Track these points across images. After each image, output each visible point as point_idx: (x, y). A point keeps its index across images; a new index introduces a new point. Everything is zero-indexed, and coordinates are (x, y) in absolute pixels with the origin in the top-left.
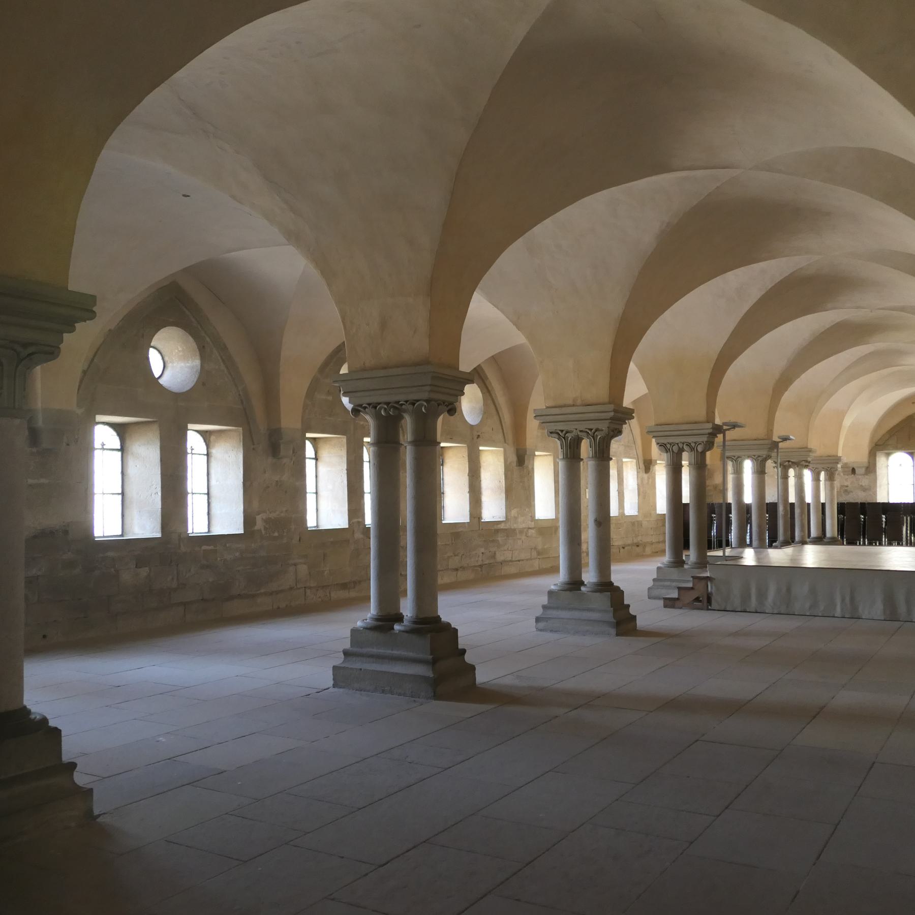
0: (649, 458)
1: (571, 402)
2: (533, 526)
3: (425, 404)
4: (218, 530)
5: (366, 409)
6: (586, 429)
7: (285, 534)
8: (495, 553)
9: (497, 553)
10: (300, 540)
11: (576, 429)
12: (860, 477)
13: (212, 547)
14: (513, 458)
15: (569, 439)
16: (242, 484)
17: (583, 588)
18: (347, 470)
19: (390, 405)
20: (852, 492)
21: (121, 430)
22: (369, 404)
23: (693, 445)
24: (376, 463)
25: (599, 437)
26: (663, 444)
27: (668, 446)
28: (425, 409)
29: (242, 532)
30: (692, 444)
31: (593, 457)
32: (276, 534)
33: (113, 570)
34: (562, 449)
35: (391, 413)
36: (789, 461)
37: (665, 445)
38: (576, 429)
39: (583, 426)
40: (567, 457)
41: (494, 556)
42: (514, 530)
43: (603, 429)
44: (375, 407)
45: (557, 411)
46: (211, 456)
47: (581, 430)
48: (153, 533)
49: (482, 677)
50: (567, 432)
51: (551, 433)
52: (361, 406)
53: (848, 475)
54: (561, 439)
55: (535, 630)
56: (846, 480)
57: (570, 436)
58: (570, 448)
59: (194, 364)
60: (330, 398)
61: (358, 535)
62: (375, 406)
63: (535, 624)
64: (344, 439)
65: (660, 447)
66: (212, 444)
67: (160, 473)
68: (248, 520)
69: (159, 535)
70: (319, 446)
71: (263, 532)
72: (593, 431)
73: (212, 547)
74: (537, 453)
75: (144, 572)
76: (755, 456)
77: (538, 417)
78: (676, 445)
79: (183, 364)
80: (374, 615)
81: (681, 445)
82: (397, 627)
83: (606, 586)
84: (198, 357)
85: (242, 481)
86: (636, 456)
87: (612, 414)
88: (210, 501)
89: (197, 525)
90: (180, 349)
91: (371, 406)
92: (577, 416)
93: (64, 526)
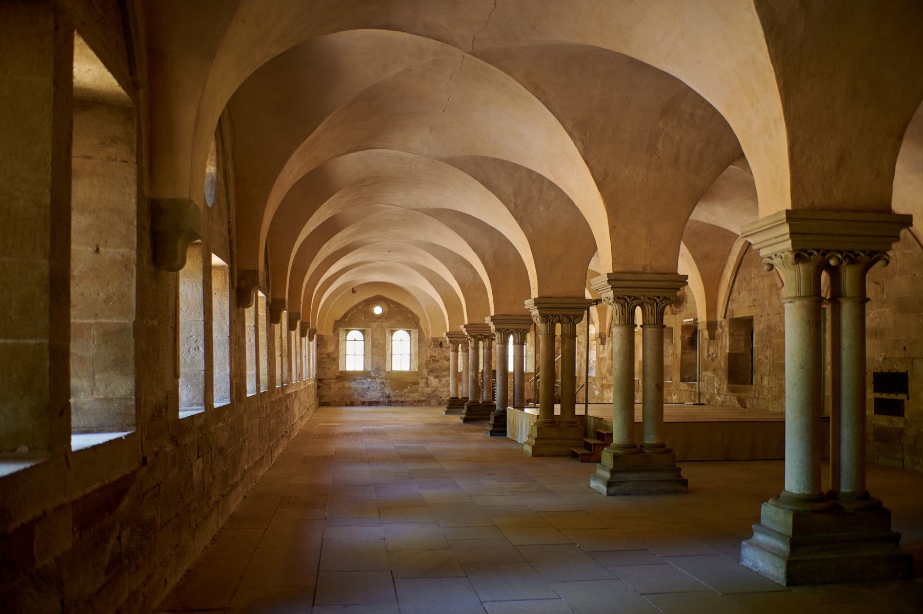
1: (640, 270)
6: (654, 296)
11: (645, 296)
12: (445, 349)
19: (844, 255)
20: (438, 361)
23: (572, 317)
24: (811, 320)
26: (546, 315)
30: (571, 317)
34: (623, 314)
36: (482, 335)
38: (645, 296)
43: (670, 297)
44: (824, 255)
45: (632, 277)
48: (192, 405)
51: (618, 298)
52: (805, 251)
53: (436, 348)
56: (435, 351)
76: (521, 329)
77: (612, 282)
78: (557, 317)
80: (809, 495)
81: (561, 317)
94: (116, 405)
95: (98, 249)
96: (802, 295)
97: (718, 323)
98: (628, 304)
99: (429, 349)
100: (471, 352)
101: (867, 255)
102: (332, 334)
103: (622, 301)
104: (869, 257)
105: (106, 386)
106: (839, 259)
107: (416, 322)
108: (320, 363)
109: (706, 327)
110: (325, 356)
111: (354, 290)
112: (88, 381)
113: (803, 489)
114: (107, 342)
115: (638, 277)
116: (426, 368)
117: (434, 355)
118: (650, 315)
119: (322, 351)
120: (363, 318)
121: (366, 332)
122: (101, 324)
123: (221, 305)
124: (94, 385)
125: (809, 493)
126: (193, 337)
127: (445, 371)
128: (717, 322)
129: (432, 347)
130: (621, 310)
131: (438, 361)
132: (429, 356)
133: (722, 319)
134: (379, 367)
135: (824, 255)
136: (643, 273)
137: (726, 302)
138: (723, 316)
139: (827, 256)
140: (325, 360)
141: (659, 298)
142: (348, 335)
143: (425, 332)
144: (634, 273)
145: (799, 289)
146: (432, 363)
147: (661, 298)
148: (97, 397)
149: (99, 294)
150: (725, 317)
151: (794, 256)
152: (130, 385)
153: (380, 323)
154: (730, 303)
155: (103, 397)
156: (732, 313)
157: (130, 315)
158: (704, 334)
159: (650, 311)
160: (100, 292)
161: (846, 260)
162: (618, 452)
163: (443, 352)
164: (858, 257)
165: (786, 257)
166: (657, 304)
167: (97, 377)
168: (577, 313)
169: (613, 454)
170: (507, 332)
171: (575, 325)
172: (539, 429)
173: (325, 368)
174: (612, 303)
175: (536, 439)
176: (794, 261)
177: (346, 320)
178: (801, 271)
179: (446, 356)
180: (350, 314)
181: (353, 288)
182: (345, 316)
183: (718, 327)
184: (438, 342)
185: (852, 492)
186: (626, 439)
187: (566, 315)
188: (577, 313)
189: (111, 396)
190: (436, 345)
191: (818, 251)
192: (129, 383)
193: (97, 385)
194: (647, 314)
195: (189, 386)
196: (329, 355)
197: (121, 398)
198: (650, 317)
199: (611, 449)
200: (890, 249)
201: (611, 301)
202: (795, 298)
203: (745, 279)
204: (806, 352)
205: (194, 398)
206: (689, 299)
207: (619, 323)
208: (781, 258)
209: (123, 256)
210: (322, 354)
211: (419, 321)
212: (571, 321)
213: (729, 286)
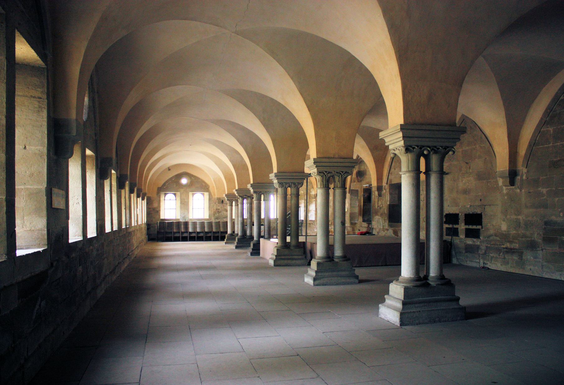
6: (340, 171)
11: (334, 171)
12: (225, 205)
16: (95, 198)
17: (336, 260)
19: (431, 148)
23: (297, 184)
24: (414, 183)
26: (281, 183)
27: (284, 184)
31: (340, 187)
36: (246, 195)
38: (334, 171)
39: (339, 170)
40: (326, 187)
44: (421, 148)
47: (337, 172)
48: (76, 236)
51: (320, 172)
52: (411, 146)
53: (219, 204)
54: (323, 177)
56: (219, 206)
65: (280, 184)
80: (413, 278)
85: (95, 196)
91: (419, 147)
92: (337, 164)
94: (36, 234)
95: (25, 147)
96: (410, 170)
97: (383, 187)
98: (325, 176)
99: (215, 205)
100: (240, 206)
101: (443, 149)
102: (156, 196)
103: (322, 174)
104: (445, 150)
105: (31, 223)
106: (428, 150)
107: (207, 189)
108: (149, 214)
109: (376, 190)
110: (152, 209)
111: (170, 168)
112: (20, 220)
113: (410, 275)
114: (31, 199)
115: (331, 160)
116: (213, 217)
117: (218, 208)
118: (338, 182)
119: (150, 207)
120: (175, 186)
121: (177, 195)
122: (27, 189)
123: (91, 178)
124: (24, 222)
126: (76, 197)
127: (225, 218)
128: (382, 186)
129: (217, 203)
130: (321, 179)
131: (221, 212)
132: (215, 209)
133: (385, 185)
134: (185, 216)
135: (421, 148)
136: (334, 158)
137: (388, 175)
138: (386, 183)
139: (423, 149)
140: (152, 212)
141: (343, 172)
142: (166, 196)
143: (212, 194)
144: (329, 158)
145: (408, 167)
146: (217, 213)
147: (344, 173)
148: (26, 229)
149: (26, 172)
150: (387, 184)
151: (405, 149)
152: (43, 223)
153: (185, 189)
154: (390, 174)
155: (29, 229)
156: (391, 181)
157: (44, 183)
158: (375, 193)
159: (338, 180)
160: (27, 171)
161: (433, 151)
162: (319, 261)
163: (224, 206)
164: (439, 150)
165: (402, 150)
166: (342, 176)
167: (25, 218)
168: (300, 181)
169: (317, 262)
170: (260, 193)
171: (299, 188)
172: (278, 250)
173: (151, 217)
174: (316, 175)
175: (276, 256)
176: (405, 152)
177: (164, 187)
178: (409, 158)
179: (225, 209)
180: (167, 184)
181: (169, 168)
182: (164, 185)
183: (383, 189)
184: (220, 200)
185: (436, 276)
186: (324, 253)
187: (293, 183)
188: (300, 181)
189: (33, 229)
190: (219, 202)
191: (418, 146)
192: (43, 221)
193: (25, 222)
194: (336, 182)
195: (74, 225)
196: (154, 209)
197: (39, 230)
198: (338, 184)
199: (316, 259)
200: (455, 145)
201: (316, 174)
202: (406, 171)
203: (398, 161)
204: (412, 201)
206: (367, 173)
207: (320, 187)
208: (399, 150)
209: (39, 151)
210: (150, 208)
211: (209, 187)
212: (296, 186)
213: (389, 165)
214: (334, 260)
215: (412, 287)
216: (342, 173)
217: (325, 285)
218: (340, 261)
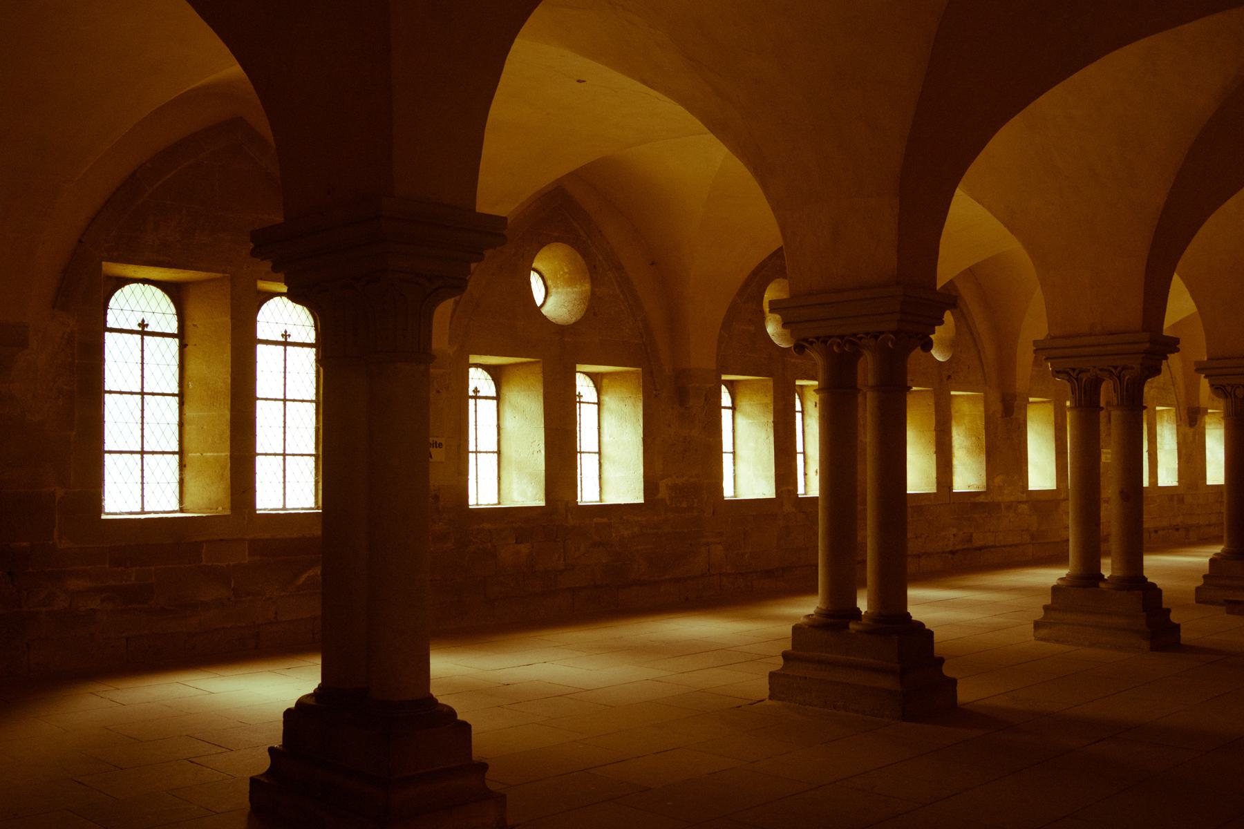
0: (1197, 406)
2: (1025, 500)
3: (892, 336)
4: (611, 499)
5: (814, 345)
7: (695, 505)
8: (971, 536)
9: (974, 535)
10: (713, 513)
13: (605, 520)
14: (997, 407)
15: (1084, 380)
16: (641, 440)
17: (1102, 585)
18: (774, 422)
21: (496, 373)
22: (818, 338)
25: (1127, 378)
26: (1221, 385)
27: (1229, 389)
28: (892, 344)
29: (641, 500)
32: (684, 505)
33: (489, 544)
34: (1073, 394)
35: (846, 349)
37: (1224, 387)
38: (1094, 367)
41: (970, 540)
42: (998, 505)
44: (825, 342)
46: (603, 405)
49: (966, 693)
50: (1081, 371)
52: (806, 340)
55: (1033, 638)
57: (1084, 377)
58: (1084, 393)
59: (584, 289)
60: (752, 328)
61: (788, 508)
62: (824, 340)
63: (1033, 630)
64: (769, 381)
66: (604, 389)
67: (543, 426)
68: (650, 485)
69: (542, 503)
70: (737, 391)
71: (668, 502)
72: (1119, 369)
73: (605, 520)
74: (1031, 399)
75: (524, 549)
79: (569, 289)
80: (821, 609)
82: (853, 626)
83: (1134, 580)
84: (588, 280)
85: (642, 436)
86: (1176, 402)
87: (1148, 345)
88: (602, 461)
89: (588, 494)
90: (566, 270)
93: (434, 490)
125: (824, 608)
135: (825, 342)
147: (1119, 369)
205: (536, 494)
214: (1098, 586)
215: (807, 627)
216: (1071, 372)
217: (1062, 642)
218: (1109, 588)
